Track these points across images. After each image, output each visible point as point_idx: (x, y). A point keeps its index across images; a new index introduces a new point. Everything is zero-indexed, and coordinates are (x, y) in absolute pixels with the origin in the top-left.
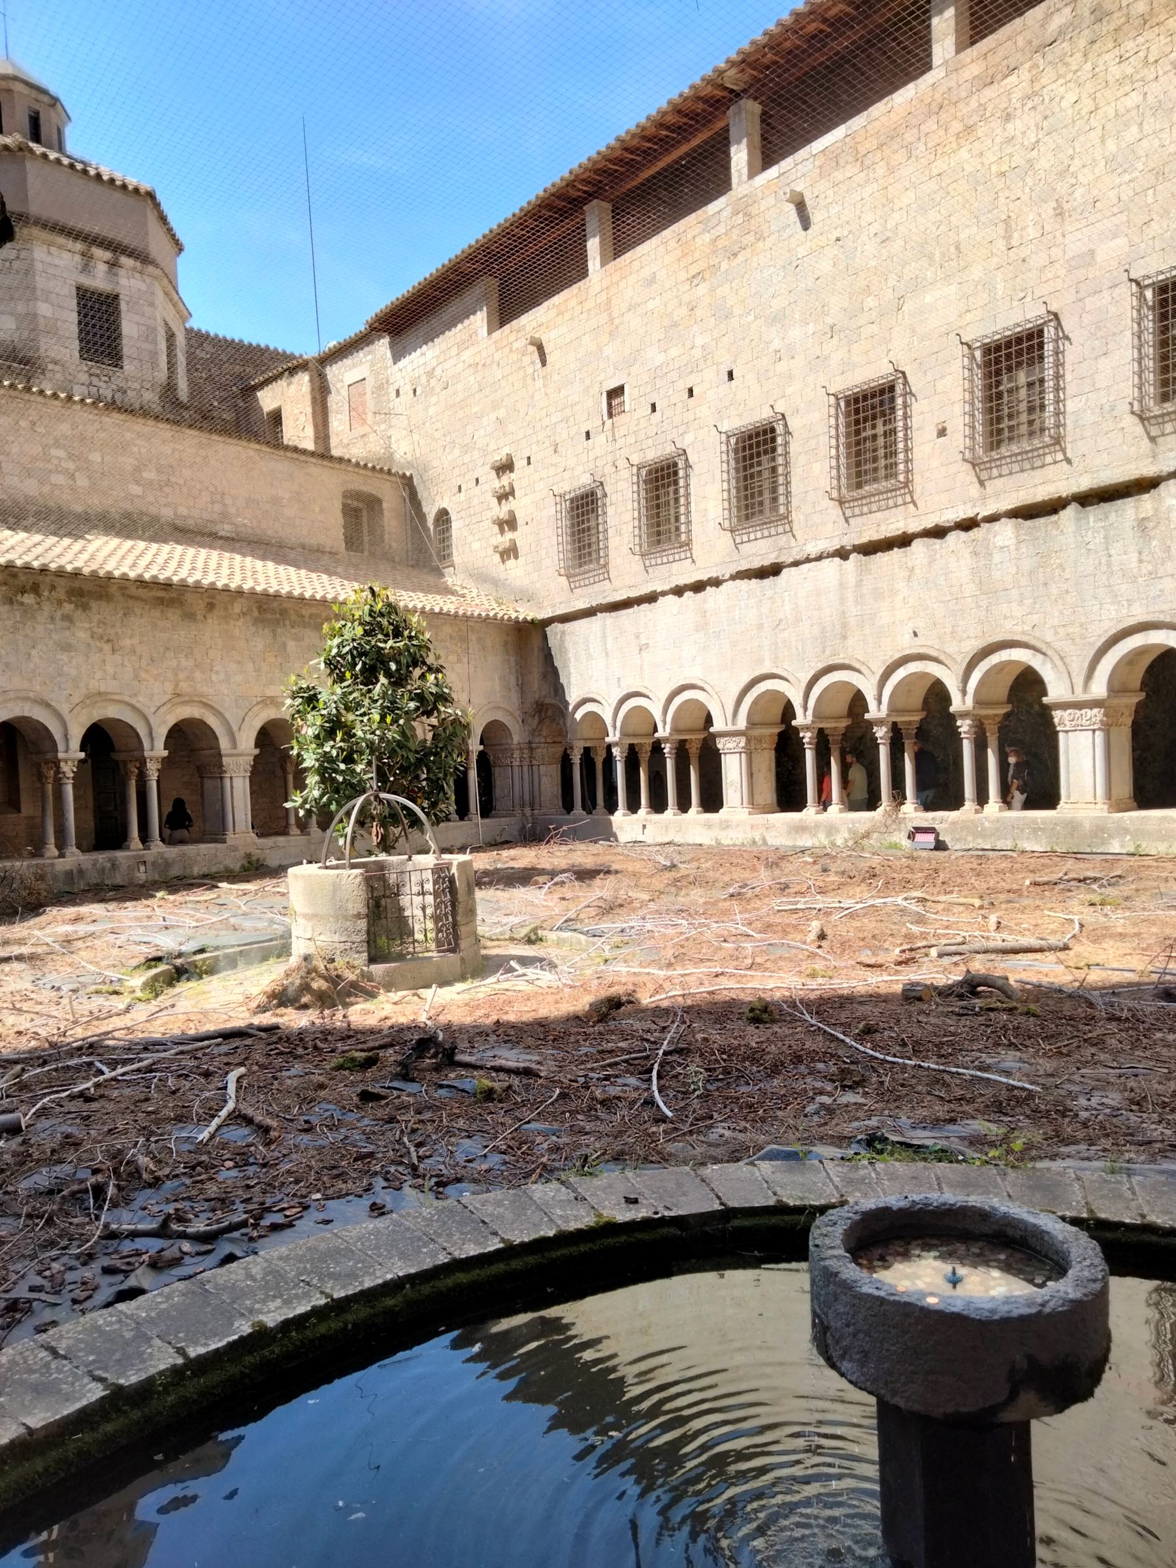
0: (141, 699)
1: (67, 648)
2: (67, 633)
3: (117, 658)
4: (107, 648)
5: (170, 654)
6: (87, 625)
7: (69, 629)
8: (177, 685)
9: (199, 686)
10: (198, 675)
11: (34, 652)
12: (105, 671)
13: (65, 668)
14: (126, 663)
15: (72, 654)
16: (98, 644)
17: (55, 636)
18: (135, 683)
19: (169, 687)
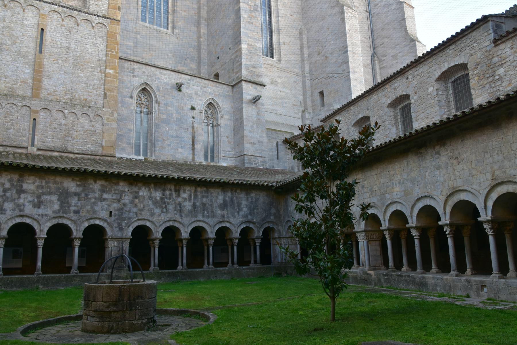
0: (474, 187)
1: (438, 168)
2: (438, 160)
3: (460, 166)
4: (455, 162)
5: (488, 156)
6: (445, 153)
7: (438, 158)
8: (493, 174)
9: (508, 171)
10: (506, 163)
11: (427, 174)
12: (455, 175)
13: (439, 178)
14: (465, 168)
15: (441, 170)
16: (451, 161)
17: (434, 163)
18: (470, 178)
19: (489, 176)
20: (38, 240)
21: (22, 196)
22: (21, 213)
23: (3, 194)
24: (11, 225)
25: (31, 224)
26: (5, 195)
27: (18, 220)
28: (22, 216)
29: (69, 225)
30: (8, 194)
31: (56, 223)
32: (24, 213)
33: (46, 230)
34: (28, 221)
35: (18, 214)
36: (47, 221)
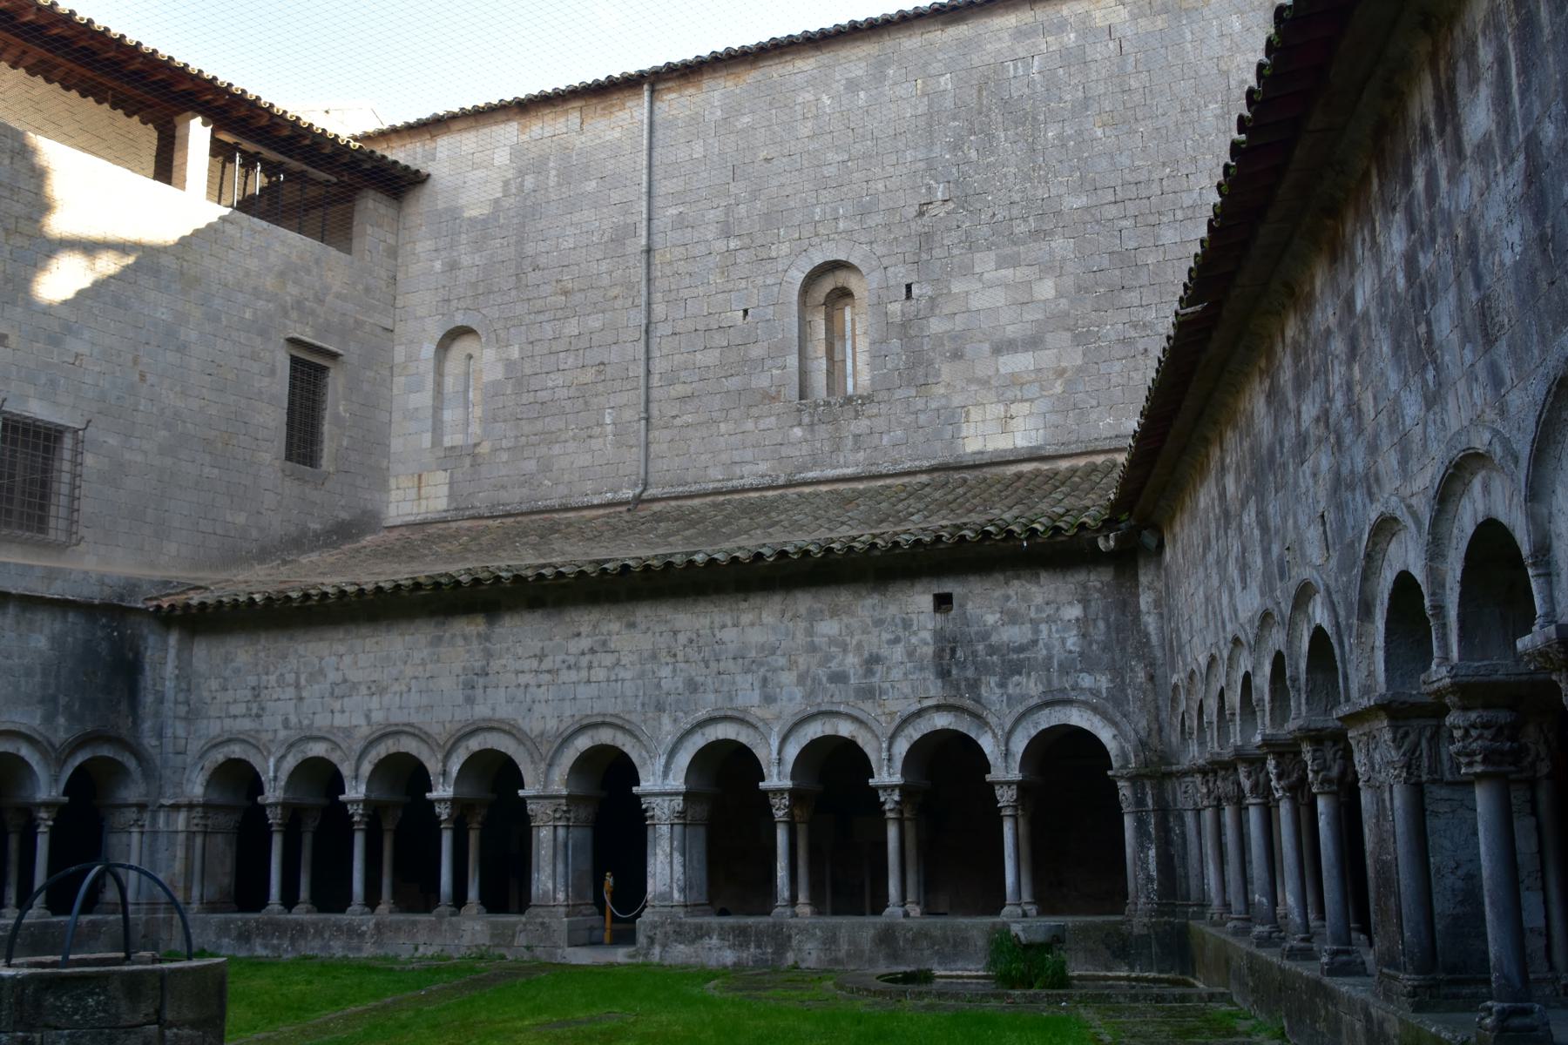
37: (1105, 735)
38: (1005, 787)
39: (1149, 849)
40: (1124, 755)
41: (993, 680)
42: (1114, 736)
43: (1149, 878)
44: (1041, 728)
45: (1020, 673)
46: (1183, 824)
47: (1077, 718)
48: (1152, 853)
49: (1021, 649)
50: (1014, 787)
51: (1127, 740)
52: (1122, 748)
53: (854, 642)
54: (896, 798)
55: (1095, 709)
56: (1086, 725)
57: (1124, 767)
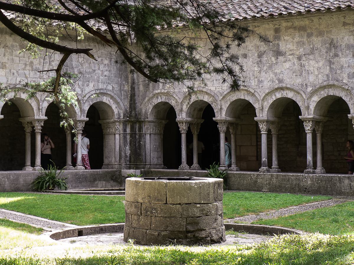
20: (305, 124)
21: (281, 58)
22: (280, 85)
23: (259, 59)
24: (271, 101)
25: (294, 99)
26: (260, 61)
27: (279, 95)
28: (282, 89)
29: (343, 98)
30: (264, 59)
31: (326, 95)
32: (284, 85)
33: (312, 106)
34: (290, 95)
35: (276, 87)
36: (314, 92)
37: (114, 107)
38: (81, 123)
39: (127, 146)
40: (119, 114)
41: (80, 83)
42: (116, 107)
43: (126, 156)
44: (94, 102)
45: (89, 82)
46: (145, 139)
47: (105, 99)
48: (127, 148)
49: (89, 73)
50: (84, 123)
51: (121, 109)
52: (118, 111)
53: (29, 61)
54: (43, 125)
55: (112, 97)
56: (108, 102)
57: (119, 118)
